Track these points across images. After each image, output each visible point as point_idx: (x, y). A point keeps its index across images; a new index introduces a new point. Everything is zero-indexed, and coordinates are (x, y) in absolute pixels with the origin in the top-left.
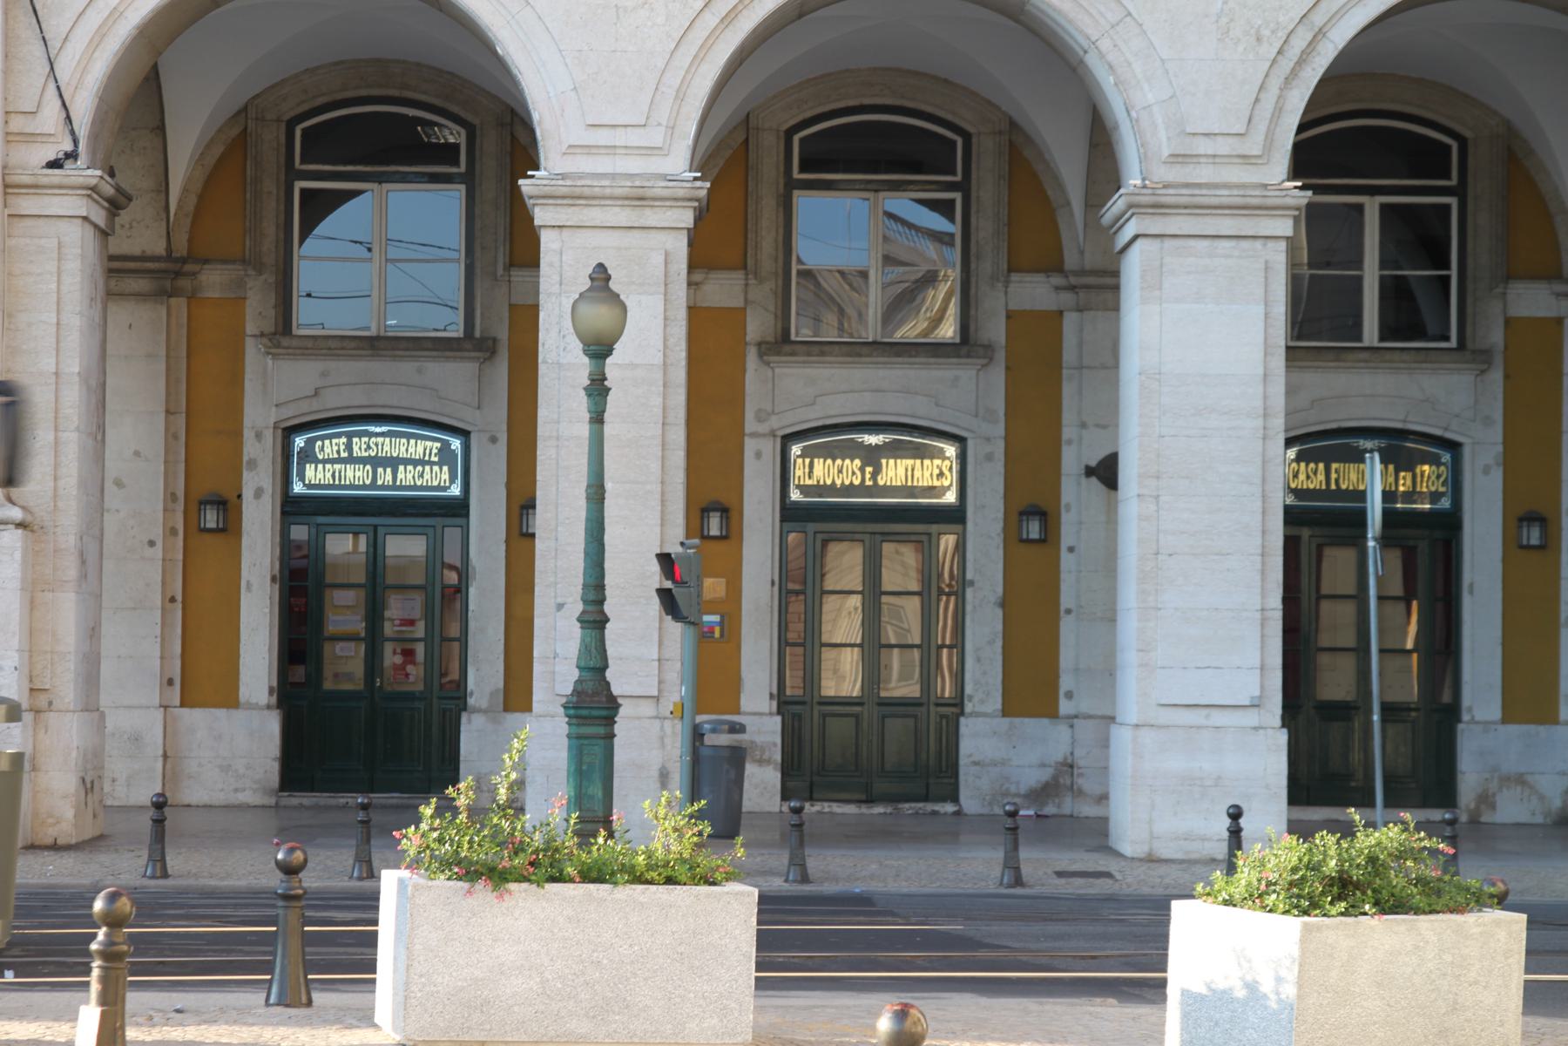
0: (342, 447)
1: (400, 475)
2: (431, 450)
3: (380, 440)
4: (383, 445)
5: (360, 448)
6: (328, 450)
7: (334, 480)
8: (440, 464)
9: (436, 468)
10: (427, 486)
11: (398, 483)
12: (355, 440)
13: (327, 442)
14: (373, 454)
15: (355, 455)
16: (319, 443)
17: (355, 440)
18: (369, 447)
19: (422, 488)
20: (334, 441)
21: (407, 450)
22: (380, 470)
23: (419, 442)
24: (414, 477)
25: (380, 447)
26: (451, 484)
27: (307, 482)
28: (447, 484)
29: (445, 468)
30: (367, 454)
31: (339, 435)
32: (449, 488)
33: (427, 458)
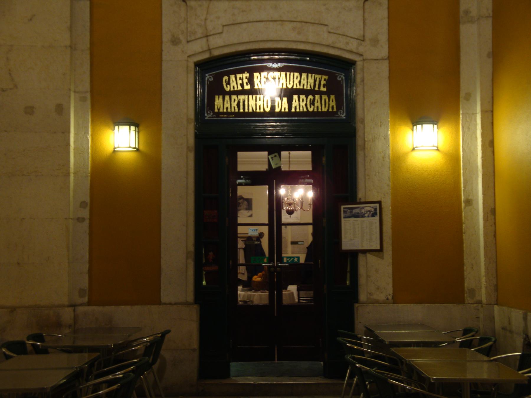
0: (245, 81)
1: (295, 103)
2: (320, 82)
5: (260, 82)
6: (233, 84)
8: (328, 93)
9: (324, 97)
10: (318, 112)
11: (293, 110)
12: (256, 74)
13: (232, 77)
16: (225, 78)
17: (256, 74)
20: (239, 76)
23: (310, 75)
27: (216, 110)
28: (335, 110)
29: (332, 97)
31: (242, 71)
33: (316, 89)
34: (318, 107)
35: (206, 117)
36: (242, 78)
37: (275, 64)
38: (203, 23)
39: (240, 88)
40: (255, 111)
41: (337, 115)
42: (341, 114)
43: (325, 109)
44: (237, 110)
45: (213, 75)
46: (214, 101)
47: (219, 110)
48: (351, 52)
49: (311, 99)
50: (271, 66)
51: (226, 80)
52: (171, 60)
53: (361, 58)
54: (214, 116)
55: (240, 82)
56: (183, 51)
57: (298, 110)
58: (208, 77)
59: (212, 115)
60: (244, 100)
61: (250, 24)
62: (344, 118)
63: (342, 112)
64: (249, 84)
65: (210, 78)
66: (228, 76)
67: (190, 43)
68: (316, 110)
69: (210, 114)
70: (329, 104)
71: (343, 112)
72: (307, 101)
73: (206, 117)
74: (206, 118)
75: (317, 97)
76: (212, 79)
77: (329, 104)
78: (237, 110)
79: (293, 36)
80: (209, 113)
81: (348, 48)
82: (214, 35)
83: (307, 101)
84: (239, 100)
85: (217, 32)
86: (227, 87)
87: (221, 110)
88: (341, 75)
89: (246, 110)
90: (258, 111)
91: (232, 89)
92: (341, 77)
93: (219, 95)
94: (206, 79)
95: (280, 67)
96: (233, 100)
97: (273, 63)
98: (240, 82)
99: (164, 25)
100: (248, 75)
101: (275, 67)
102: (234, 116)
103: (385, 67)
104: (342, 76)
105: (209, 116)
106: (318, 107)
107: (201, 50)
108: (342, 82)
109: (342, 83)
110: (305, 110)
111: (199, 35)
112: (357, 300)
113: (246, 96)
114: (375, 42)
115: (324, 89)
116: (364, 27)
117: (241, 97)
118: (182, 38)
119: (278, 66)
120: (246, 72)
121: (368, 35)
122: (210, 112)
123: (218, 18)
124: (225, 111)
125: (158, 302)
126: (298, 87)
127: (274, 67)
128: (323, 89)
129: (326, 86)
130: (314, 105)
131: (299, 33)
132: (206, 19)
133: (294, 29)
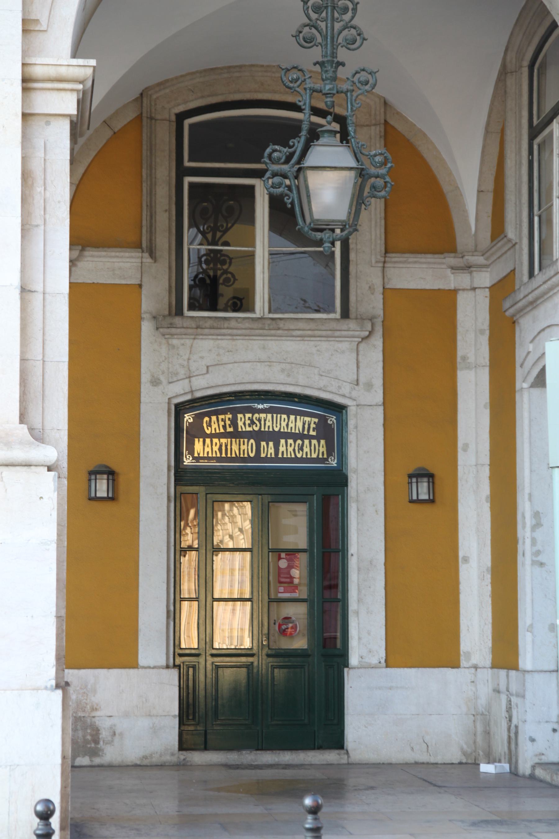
0: (228, 422)
1: (282, 449)
2: (309, 425)
3: (263, 416)
4: (265, 420)
5: (244, 424)
6: (215, 426)
7: (221, 453)
8: (318, 438)
9: (314, 442)
11: (280, 456)
12: (240, 416)
13: (214, 418)
14: (256, 429)
15: (240, 430)
16: (206, 419)
17: (240, 416)
18: (252, 423)
19: (302, 460)
20: (221, 417)
21: (287, 425)
22: (263, 444)
23: (298, 417)
24: (294, 450)
25: (263, 422)
26: (328, 456)
27: (196, 455)
28: (325, 456)
29: (323, 442)
30: (251, 429)
31: (224, 412)
32: (327, 459)
33: (306, 432)
34: (307, 453)
36: (224, 419)
37: (260, 404)
38: (185, 363)
39: (222, 430)
40: (238, 455)
41: (327, 462)
42: (331, 460)
43: (314, 456)
44: (218, 455)
45: (192, 416)
46: (194, 444)
47: (199, 454)
48: (344, 396)
49: (299, 444)
50: (256, 407)
51: (207, 421)
52: (151, 403)
53: (355, 403)
54: (193, 461)
55: (223, 423)
56: (163, 393)
57: (285, 456)
58: (187, 418)
59: (192, 460)
60: (226, 444)
61: (236, 364)
62: (336, 465)
63: (333, 458)
64: (231, 425)
65: (190, 419)
66: (209, 417)
67: (171, 385)
68: (304, 456)
69: (189, 459)
70: (319, 450)
71: (335, 458)
72: (295, 446)
73: (185, 462)
77: (319, 450)
78: (218, 455)
79: (282, 378)
80: (188, 457)
81: (341, 392)
82: (197, 375)
83: (295, 446)
84: (221, 444)
85: (201, 373)
86: (208, 429)
87: (201, 455)
88: (332, 418)
89: (229, 455)
90: (242, 456)
91: (213, 432)
92: (332, 420)
93: (199, 438)
95: (266, 408)
96: (214, 444)
97: (259, 404)
98: (223, 423)
99: (143, 364)
100: (230, 416)
101: (261, 408)
102: (215, 461)
103: (379, 413)
104: (333, 419)
105: (188, 461)
106: (307, 453)
107: (182, 392)
108: (333, 425)
109: (333, 427)
110: (293, 456)
111: (181, 376)
112: (347, 665)
113: (229, 440)
114: (369, 386)
115: (314, 433)
116: (357, 370)
117: (223, 441)
118: (162, 378)
119: (264, 407)
120: (229, 413)
121: (362, 380)
122: (189, 457)
123: (202, 358)
124: (206, 455)
125: (134, 665)
126: (286, 430)
127: (259, 408)
128: (312, 433)
129: (315, 430)
130: (302, 450)
131: (289, 376)
132: (189, 359)
133: (283, 370)
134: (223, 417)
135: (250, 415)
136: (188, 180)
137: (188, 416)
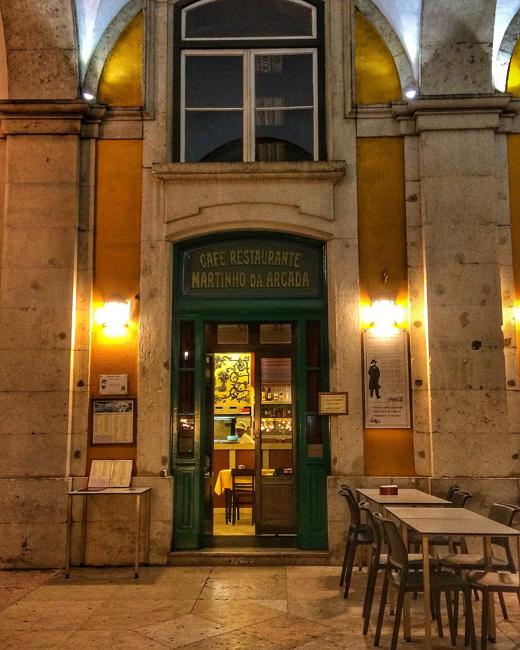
7: (215, 285)
18: (243, 258)
21: (274, 260)
25: (252, 258)
27: (193, 286)
29: (305, 273)
35: (183, 293)
39: (216, 265)
51: (203, 257)
73: (183, 293)
74: (184, 294)
75: (291, 273)
76: (190, 257)
87: (198, 286)
94: (184, 256)
104: (315, 254)
122: (187, 288)
134: (217, 253)
135: (241, 252)
136: (185, 53)
137: (187, 253)
